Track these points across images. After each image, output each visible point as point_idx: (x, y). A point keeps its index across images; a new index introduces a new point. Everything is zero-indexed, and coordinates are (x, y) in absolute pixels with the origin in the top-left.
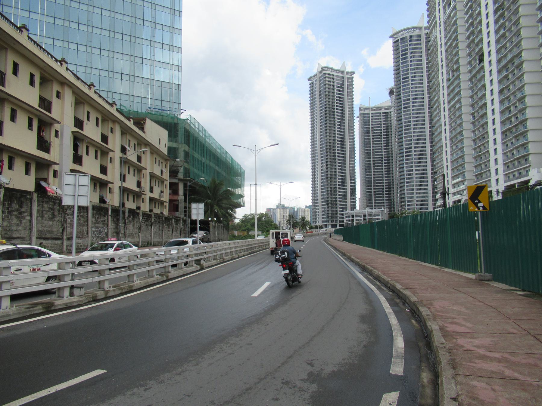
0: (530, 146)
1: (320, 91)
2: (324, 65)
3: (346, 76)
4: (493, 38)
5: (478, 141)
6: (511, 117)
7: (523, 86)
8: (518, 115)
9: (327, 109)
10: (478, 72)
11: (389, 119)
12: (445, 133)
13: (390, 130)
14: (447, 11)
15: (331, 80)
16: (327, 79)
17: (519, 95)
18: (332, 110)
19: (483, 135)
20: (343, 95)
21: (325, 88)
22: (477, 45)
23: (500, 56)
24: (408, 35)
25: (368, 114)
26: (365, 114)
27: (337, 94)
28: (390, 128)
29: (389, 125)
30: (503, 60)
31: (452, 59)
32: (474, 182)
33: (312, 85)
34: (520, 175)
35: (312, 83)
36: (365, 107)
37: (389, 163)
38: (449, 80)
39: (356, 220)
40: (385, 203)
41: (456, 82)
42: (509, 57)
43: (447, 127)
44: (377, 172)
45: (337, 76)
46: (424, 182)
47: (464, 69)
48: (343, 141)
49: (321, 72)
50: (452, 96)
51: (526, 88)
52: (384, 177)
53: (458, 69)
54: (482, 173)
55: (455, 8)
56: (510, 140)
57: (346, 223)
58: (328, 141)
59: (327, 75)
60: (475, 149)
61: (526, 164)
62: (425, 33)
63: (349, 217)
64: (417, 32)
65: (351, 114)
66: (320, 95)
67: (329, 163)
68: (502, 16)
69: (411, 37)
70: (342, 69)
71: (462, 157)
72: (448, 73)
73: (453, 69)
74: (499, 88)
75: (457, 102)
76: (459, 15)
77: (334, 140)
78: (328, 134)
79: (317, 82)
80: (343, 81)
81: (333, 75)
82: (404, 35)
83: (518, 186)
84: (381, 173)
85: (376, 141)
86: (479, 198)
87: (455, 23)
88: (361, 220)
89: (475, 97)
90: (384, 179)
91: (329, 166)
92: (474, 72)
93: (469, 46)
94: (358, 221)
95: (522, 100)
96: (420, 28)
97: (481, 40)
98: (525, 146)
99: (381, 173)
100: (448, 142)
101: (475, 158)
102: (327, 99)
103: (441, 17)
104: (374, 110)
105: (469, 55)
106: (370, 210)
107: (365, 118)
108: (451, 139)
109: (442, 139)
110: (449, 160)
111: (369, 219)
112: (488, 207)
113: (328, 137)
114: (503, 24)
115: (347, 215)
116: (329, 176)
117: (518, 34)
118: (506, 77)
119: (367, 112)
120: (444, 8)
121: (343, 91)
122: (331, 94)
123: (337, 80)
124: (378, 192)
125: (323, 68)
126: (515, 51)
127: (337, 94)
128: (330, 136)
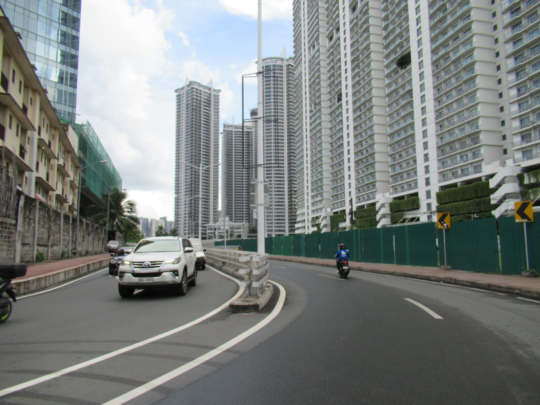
0: (377, 175)
1: (187, 105)
2: (192, 80)
3: (213, 93)
4: (350, 83)
5: (335, 167)
6: (362, 150)
7: (373, 126)
8: (368, 149)
9: (194, 122)
10: (337, 108)
11: (250, 138)
12: (307, 157)
13: (251, 149)
14: (311, 52)
15: (199, 95)
16: (194, 93)
17: (369, 133)
18: (199, 124)
19: (339, 162)
20: (210, 111)
21: (193, 102)
22: (337, 86)
23: (355, 99)
24: (271, 64)
25: (232, 131)
26: (229, 131)
27: (204, 109)
29: (251, 143)
30: (357, 102)
31: (315, 94)
32: (331, 202)
33: (179, 97)
34: (369, 199)
35: (179, 95)
36: (228, 124)
38: (311, 111)
41: (318, 115)
42: (363, 100)
43: (309, 152)
45: (204, 92)
46: (281, 198)
47: (325, 104)
48: (208, 156)
49: (188, 86)
50: (314, 125)
51: (375, 127)
53: (320, 103)
54: (338, 194)
55: (318, 50)
56: (361, 168)
57: (208, 236)
58: (194, 154)
59: (194, 90)
60: (332, 173)
61: (373, 189)
62: (286, 65)
63: (212, 229)
64: (279, 63)
65: (216, 130)
66: (187, 108)
67: (193, 176)
68: (357, 66)
69: (274, 66)
70: (210, 86)
71: (321, 180)
72: (311, 105)
73: (316, 104)
74: (354, 125)
75: (318, 131)
76: (321, 57)
77: (200, 154)
78: (194, 147)
79: (185, 95)
80: (210, 98)
81: (201, 91)
82: (268, 63)
83: (367, 207)
85: (238, 158)
86: (445, 220)
87: (318, 63)
89: (334, 129)
90: (244, 194)
91: (193, 179)
92: (333, 108)
93: (329, 85)
94: (219, 234)
95: (371, 136)
96: (282, 60)
97: (340, 82)
98: (373, 174)
99: (241, 188)
100: (309, 165)
101: (332, 181)
102: (194, 113)
103: (306, 56)
104: (237, 128)
105: (330, 93)
107: (228, 135)
108: (312, 163)
109: (303, 162)
110: (309, 182)
112: (449, 226)
113: (194, 150)
114: (358, 72)
115: (209, 228)
116: (193, 188)
117: (369, 83)
118: (359, 116)
119: (230, 129)
120: (309, 48)
121: (210, 107)
122: (198, 108)
123: (204, 95)
124: (238, 206)
125: (190, 82)
126: (367, 97)
127: (204, 109)
128: (195, 150)
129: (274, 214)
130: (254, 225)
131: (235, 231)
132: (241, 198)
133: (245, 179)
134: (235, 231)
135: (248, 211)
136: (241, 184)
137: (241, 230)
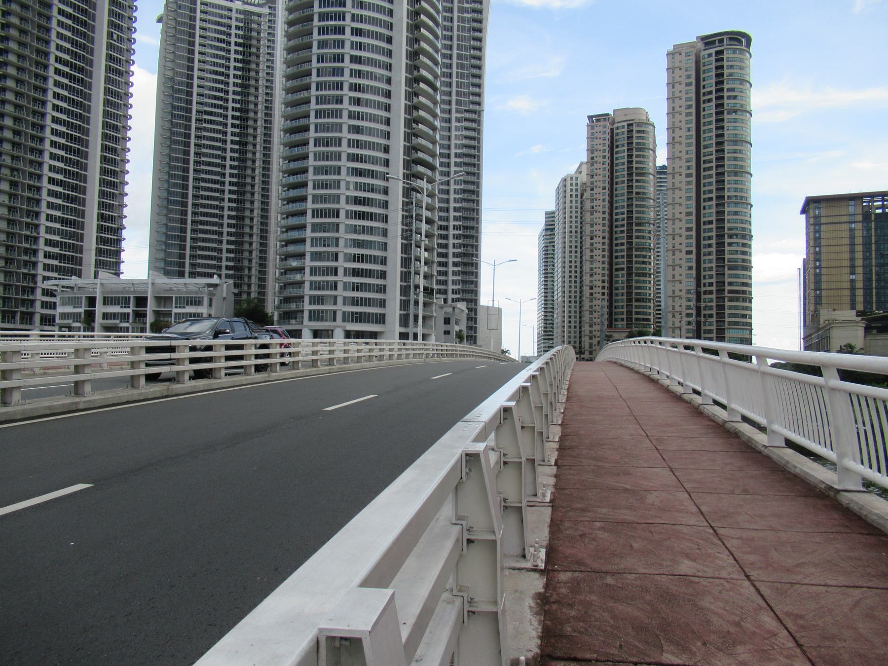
28: (253, 58)
29: (254, 50)
37: (244, 160)
40: (227, 184)
44: (205, 181)
63: (75, 302)
84: (218, 186)
88: (125, 317)
90: (226, 204)
99: (218, 186)
124: (204, 240)
131: (175, 311)
133: (232, 159)
135: (238, 260)
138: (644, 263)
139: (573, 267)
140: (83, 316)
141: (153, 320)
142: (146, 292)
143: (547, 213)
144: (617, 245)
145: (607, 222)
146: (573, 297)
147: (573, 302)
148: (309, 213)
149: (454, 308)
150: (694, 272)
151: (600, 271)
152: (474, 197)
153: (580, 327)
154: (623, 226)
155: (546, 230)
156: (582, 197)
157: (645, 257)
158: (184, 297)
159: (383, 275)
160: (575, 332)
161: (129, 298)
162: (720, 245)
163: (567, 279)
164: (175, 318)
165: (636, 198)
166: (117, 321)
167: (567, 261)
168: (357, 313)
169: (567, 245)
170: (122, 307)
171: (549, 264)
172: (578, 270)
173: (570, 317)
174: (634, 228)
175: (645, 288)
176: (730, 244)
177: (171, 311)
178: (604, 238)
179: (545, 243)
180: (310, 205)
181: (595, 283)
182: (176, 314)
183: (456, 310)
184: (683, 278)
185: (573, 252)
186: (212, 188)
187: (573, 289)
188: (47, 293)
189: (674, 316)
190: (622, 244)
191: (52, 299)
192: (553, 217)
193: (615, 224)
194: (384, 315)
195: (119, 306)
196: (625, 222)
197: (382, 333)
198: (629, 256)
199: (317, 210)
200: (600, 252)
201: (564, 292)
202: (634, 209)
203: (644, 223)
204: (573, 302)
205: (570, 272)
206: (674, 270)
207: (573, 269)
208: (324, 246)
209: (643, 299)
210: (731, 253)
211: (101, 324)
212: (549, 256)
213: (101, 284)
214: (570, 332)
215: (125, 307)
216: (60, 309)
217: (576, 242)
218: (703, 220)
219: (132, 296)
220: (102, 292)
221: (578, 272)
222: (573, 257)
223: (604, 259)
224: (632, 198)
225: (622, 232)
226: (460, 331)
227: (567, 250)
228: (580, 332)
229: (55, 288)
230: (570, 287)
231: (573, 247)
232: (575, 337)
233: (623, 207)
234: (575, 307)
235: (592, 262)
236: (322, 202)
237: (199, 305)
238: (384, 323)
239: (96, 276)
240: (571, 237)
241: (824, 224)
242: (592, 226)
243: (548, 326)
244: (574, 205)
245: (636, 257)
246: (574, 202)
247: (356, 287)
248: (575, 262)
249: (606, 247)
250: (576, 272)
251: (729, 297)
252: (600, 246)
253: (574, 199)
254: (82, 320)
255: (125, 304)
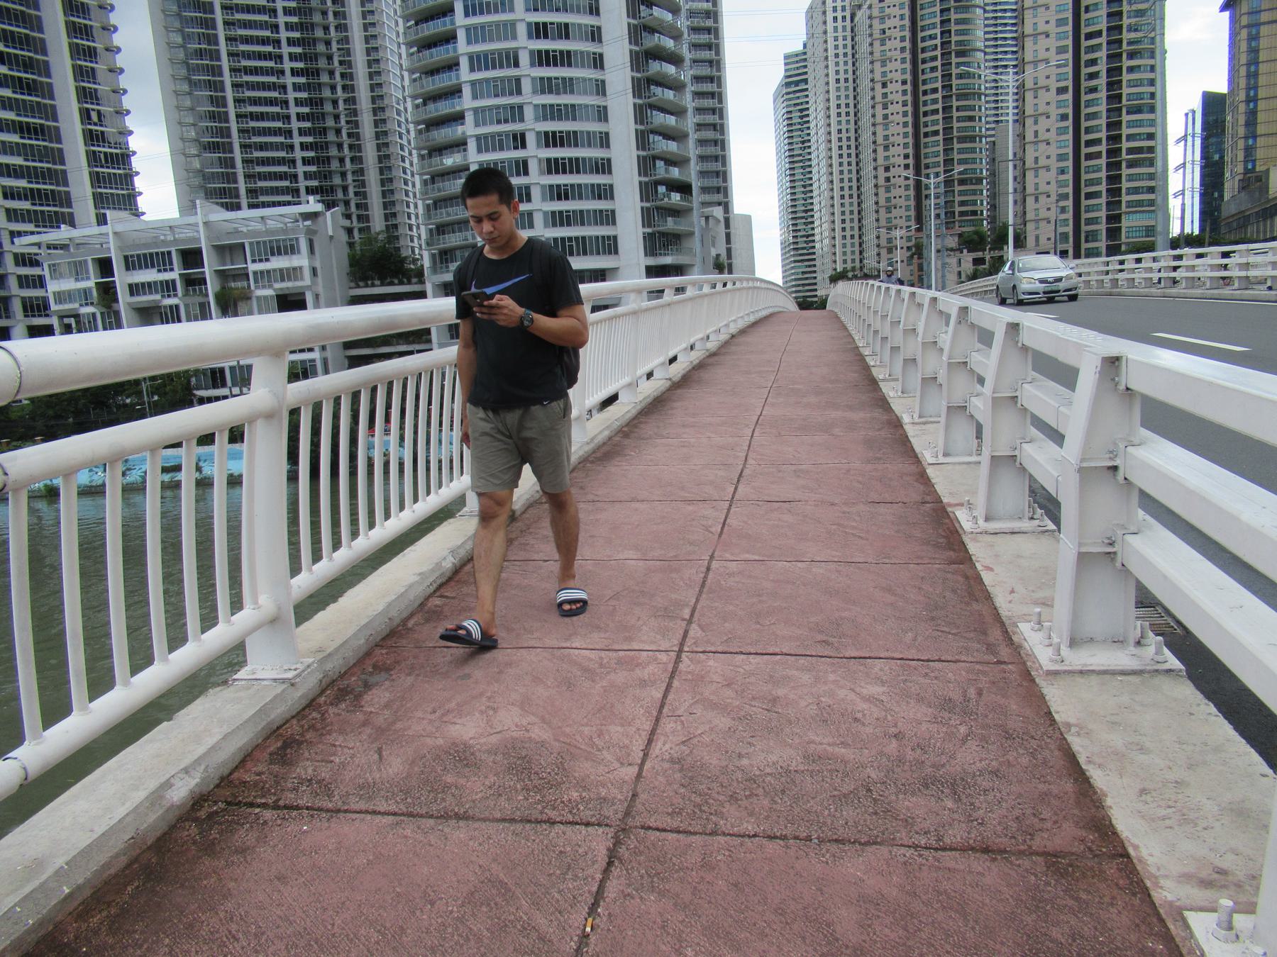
39: (134, 289)
52: (288, 73)
63: (78, 270)
88: (168, 287)
99: (269, 49)
106: (220, 215)
111: (222, 275)
124: (262, 147)
129: (532, 125)
130: (378, 224)
131: (253, 267)
132: (271, 102)
134: (253, 267)
136: (262, 25)
137: (301, 260)
138: (971, 119)
139: (844, 139)
140: (95, 293)
141: (218, 288)
142: (199, 239)
143: (786, 57)
144: (925, 93)
145: (907, 55)
146: (846, 189)
147: (847, 196)
148: (464, 63)
149: (707, 218)
150: (1069, 123)
151: (900, 140)
152: (709, 23)
153: (860, 237)
154: (934, 59)
155: (788, 85)
156: (852, 21)
157: (972, 108)
158: (265, 242)
159: (604, 167)
160: (853, 245)
161: (169, 253)
162: (1114, 72)
163: (835, 161)
164: (256, 281)
165: (956, 8)
166: (158, 297)
167: (834, 129)
168: (570, 239)
169: (833, 104)
170: (159, 271)
171: (795, 140)
172: (853, 143)
173: (843, 221)
174: (954, 60)
175: (974, 161)
176: (1131, 69)
177: (247, 268)
178: (904, 82)
179: (788, 106)
180: (463, 46)
181: (892, 160)
182: (255, 273)
183: (711, 221)
184: (1052, 136)
185: (843, 114)
186: (259, 53)
187: (846, 176)
188: (22, 260)
189: (1037, 200)
190: (935, 91)
191: (35, 271)
192: (805, 60)
193: (921, 56)
194: (615, 238)
195: (155, 270)
196: (938, 53)
197: (615, 270)
198: (947, 109)
199: (478, 57)
200: (899, 107)
201: (832, 182)
202: (953, 28)
203: (970, 50)
204: (847, 196)
205: (840, 148)
206: (1036, 123)
207: (844, 143)
208: (499, 122)
209: (971, 179)
210: (1132, 84)
211: (129, 304)
212: (794, 128)
213: (115, 233)
214: (844, 246)
215: (165, 270)
216: (53, 287)
217: (847, 97)
218: (1085, 30)
219: (173, 250)
220: (121, 248)
221: (853, 147)
222: (844, 122)
223: (905, 119)
224: (949, 9)
225: (933, 69)
226: (718, 256)
227: (833, 112)
228: (860, 245)
229: (34, 250)
230: (841, 172)
231: (843, 106)
232: (853, 252)
233: (934, 26)
234: (851, 204)
235: (886, 126)
236: (484, 41)
237: (293, 252)
238: (616, 252)
239: (102, 220)
240: (838, 89)
241: (1264, 23)
242: (884, 64)
243: (799, 240)
244: (840, 34)
245: (958, 110)
246: (840, 29)
247: (560, 193)
248: (847, 131)
249: (909, 98)
250: (849, 147)
251: (1128, 161)
252: (900, 98)
253: (840, 23)
254: (95, 301)
255: (164, 265)
